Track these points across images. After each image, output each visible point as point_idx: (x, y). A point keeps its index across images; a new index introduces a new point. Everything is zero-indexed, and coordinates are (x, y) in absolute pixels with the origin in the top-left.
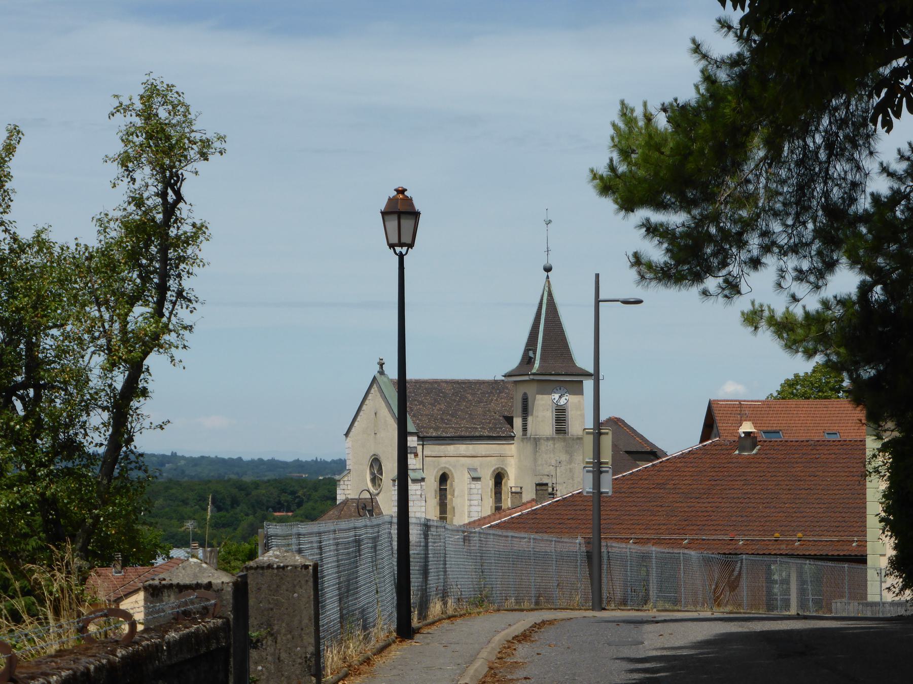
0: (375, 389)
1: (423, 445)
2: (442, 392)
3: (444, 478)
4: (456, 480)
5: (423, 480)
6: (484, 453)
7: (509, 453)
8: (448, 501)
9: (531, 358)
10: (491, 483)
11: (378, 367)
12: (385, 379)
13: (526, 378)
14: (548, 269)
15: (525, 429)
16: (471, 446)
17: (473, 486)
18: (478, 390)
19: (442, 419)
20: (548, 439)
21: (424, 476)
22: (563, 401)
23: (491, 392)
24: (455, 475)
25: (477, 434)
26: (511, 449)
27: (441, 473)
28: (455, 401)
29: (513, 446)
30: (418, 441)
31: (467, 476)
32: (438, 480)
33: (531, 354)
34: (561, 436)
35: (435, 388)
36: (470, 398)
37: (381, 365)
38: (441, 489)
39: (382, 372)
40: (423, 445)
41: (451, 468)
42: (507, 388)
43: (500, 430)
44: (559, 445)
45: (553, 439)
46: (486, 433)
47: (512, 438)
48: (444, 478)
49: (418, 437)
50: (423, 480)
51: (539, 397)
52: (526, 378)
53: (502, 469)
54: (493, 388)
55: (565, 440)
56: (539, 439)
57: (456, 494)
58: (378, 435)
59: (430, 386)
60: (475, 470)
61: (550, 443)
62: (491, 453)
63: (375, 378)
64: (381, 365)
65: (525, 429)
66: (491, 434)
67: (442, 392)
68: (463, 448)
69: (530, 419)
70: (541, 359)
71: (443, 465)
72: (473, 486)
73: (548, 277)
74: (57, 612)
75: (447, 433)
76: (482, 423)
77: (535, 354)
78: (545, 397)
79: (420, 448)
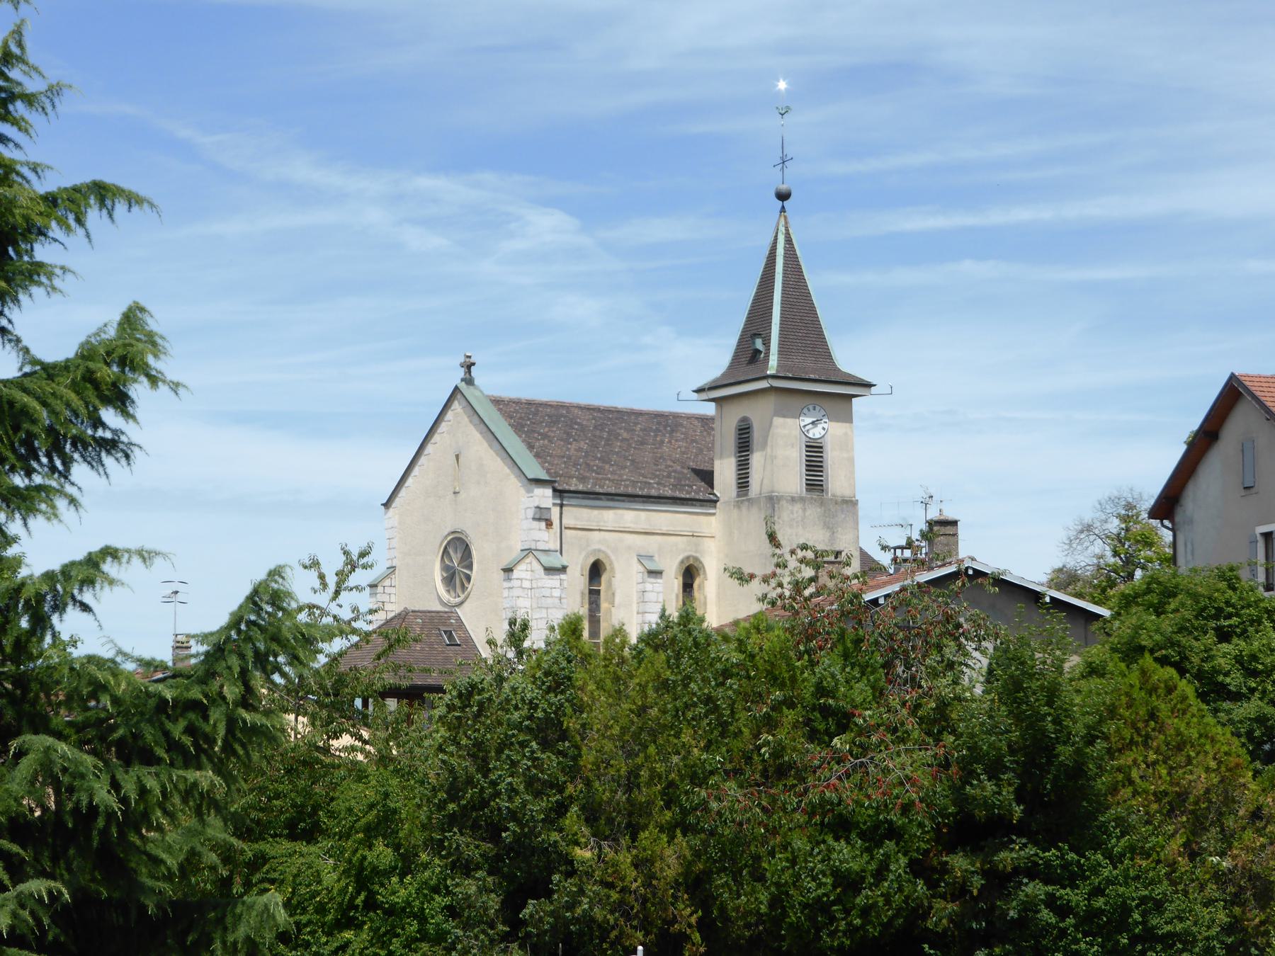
0: (456, 405)
1: (561, 506)
2: (576, 423)
3: (596, 571)
4: (618, 575)
5: (563, 569)
6: (664, 529)
7: (706, 532)
8: (602, 614)
9: (758, 352)
10: (677, 584)
11: (461, 373)
12: (478, 393)
13: (763, 384)
14: (783, 196)
15: (743, 483)
16: (643, 514)
17: (649, 587)
18: (636, 424)
19: (588, 465)
20: (793, 500)
21: (565, 563)
22: (816, 433)
23: (657, 430)
24: (616, 565)
25: (653, 492)
26: (711, 524)
27: (592, 560)
28: (601, 438)
29: (713, 518)
30: (554, 497)
31: (637, 567)
32: (587, 573)
33: (759, 344)
34: (815, 495)
35: (562, 416)
36: (625, 435)
37: (469, 366)
38: (591, 592)
39: (469, 381)
40: (561, 506)
41: (609, 552)
42: (682, 425)
43: (695, 490)
44: (813, 512)
45: (802, 499)
46: (669, 493)
47: (714, 502)
48: (596, 571)
49: (555, 490)
50: (563, 569)
51: (778, 421)
52: (763, 384)
53: (696, 559)
54: (659, 423)
55: (822, 504)
56: (779, 499)
57: (617, 600)
58: (462, 496)
59: (553, 411)
60: (651, 557)
61: (797, 507)
62: (678, 529)
63: (456, 388)
64: (469, 366)
65: (743, 483)
66: (678, 494)
67: (576, 423)
68: (630, 517)
69: (756, 459)
70: (780, 352)
71: (596, 547)
72: (649, 587)
73: (783, 209)
74: (170, 815)
75: (601, 487)
76: (657, 476)
77: (767, 343)
78: (789, 421)
79: (555, 512)
